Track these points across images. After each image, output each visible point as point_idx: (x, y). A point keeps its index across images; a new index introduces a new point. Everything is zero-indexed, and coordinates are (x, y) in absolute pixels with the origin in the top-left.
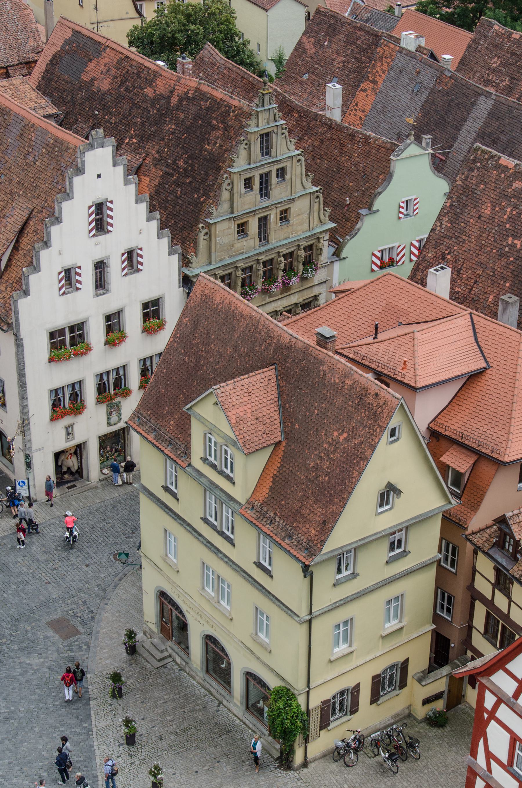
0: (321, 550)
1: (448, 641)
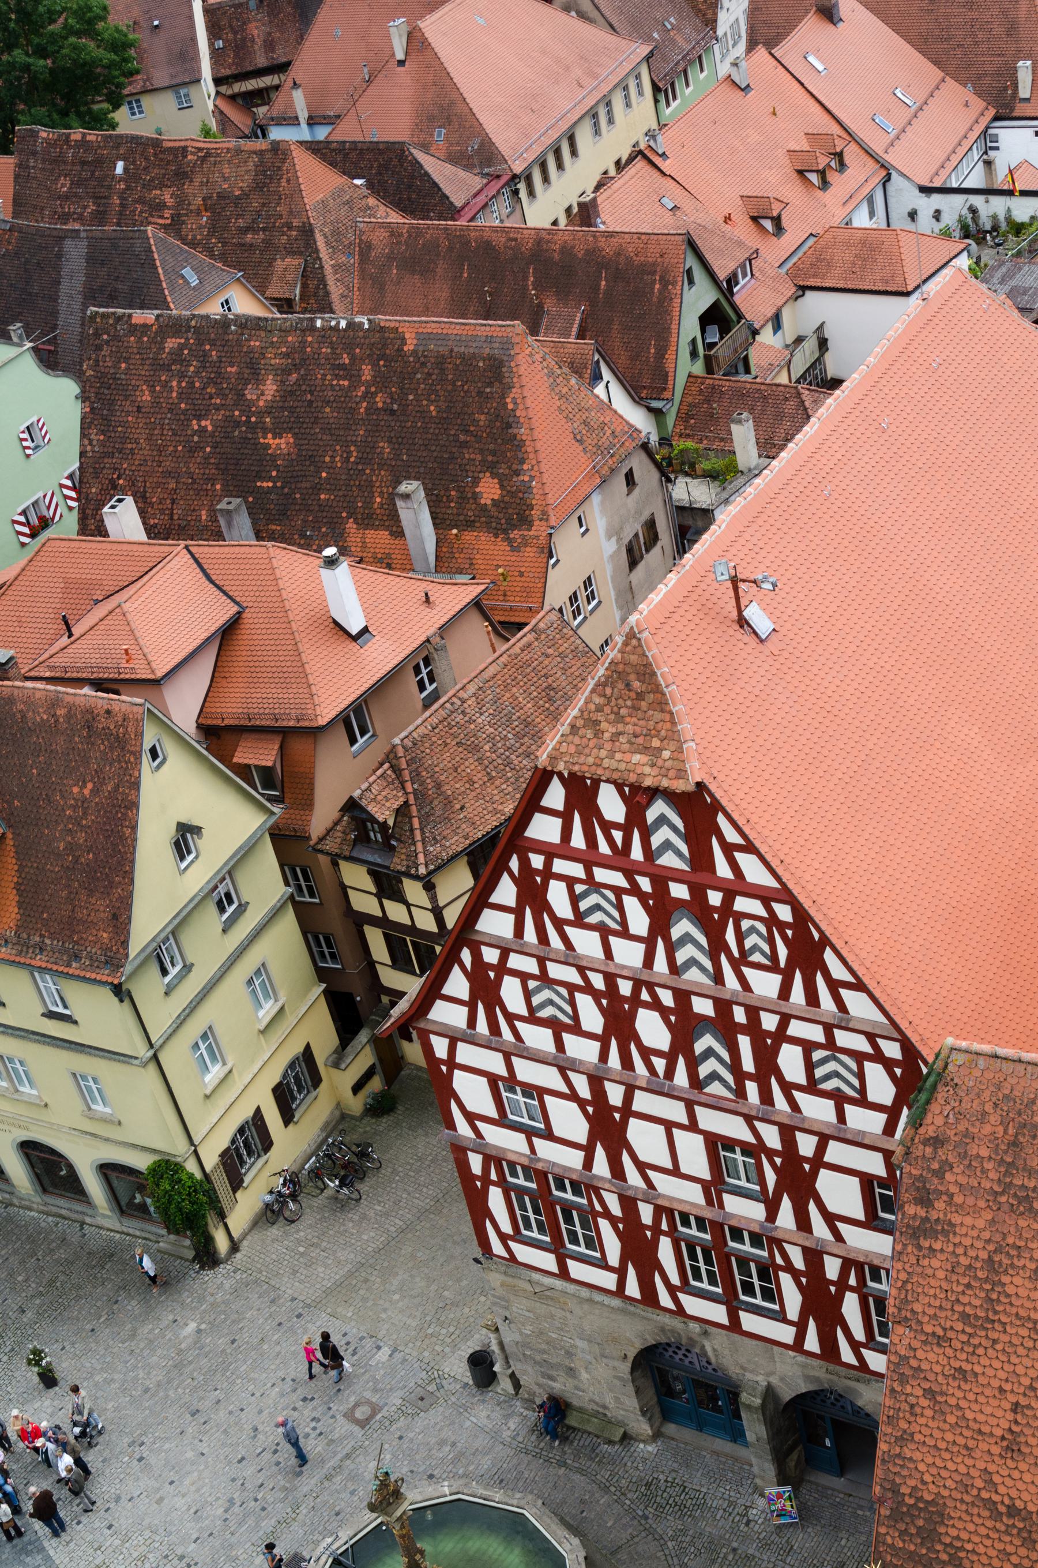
1: (350, 997)
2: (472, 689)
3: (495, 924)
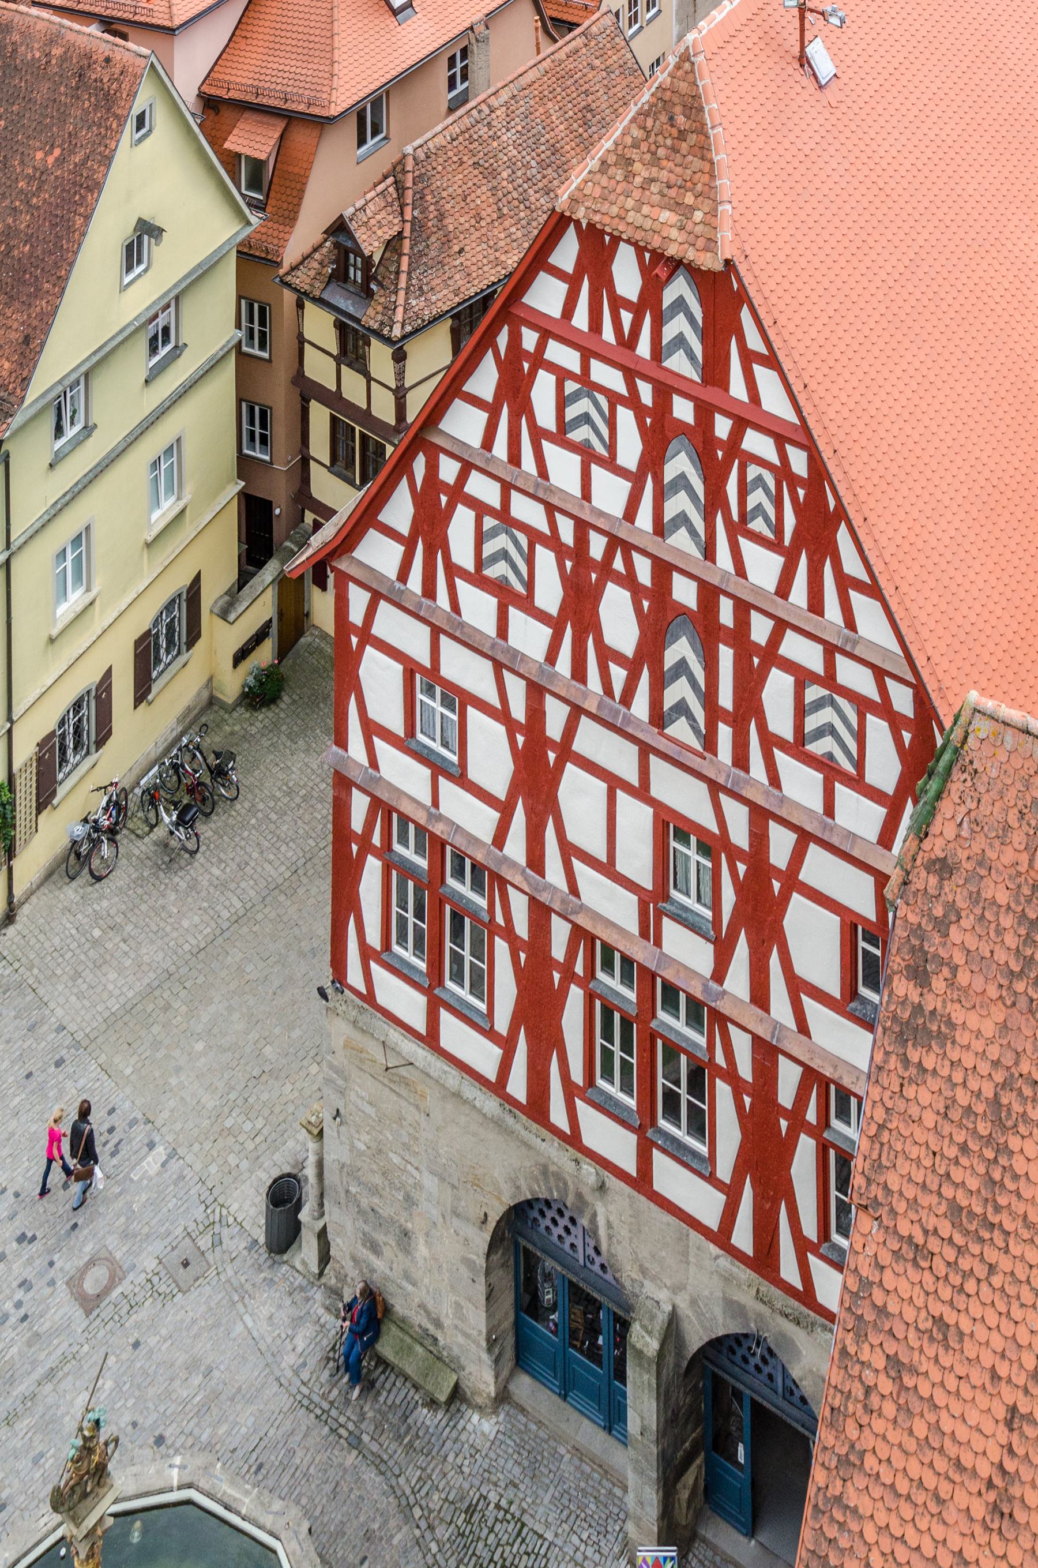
0: (23, 399)
1: (267, 506)
2: (505, 95)
3: (464, 424)
